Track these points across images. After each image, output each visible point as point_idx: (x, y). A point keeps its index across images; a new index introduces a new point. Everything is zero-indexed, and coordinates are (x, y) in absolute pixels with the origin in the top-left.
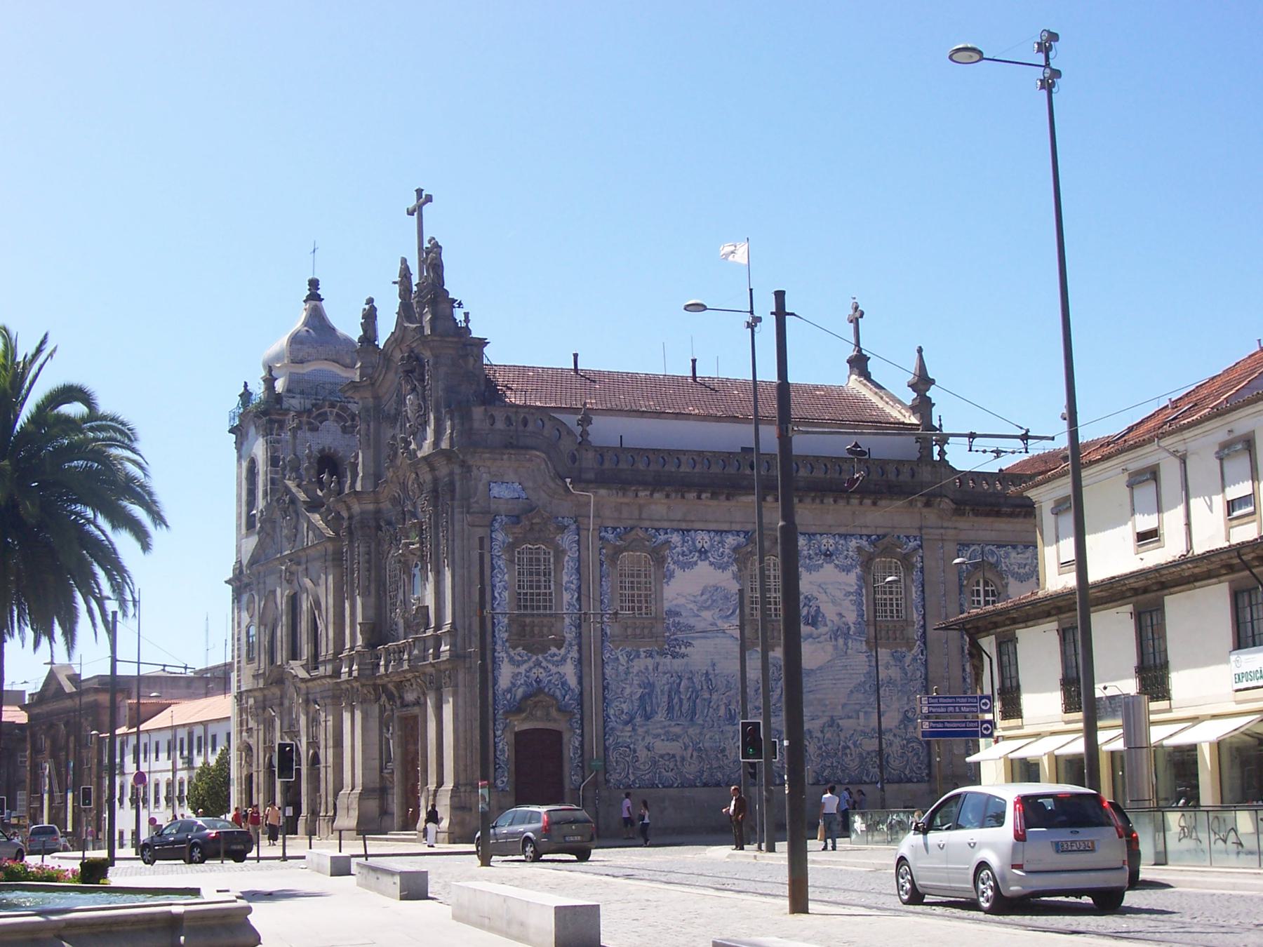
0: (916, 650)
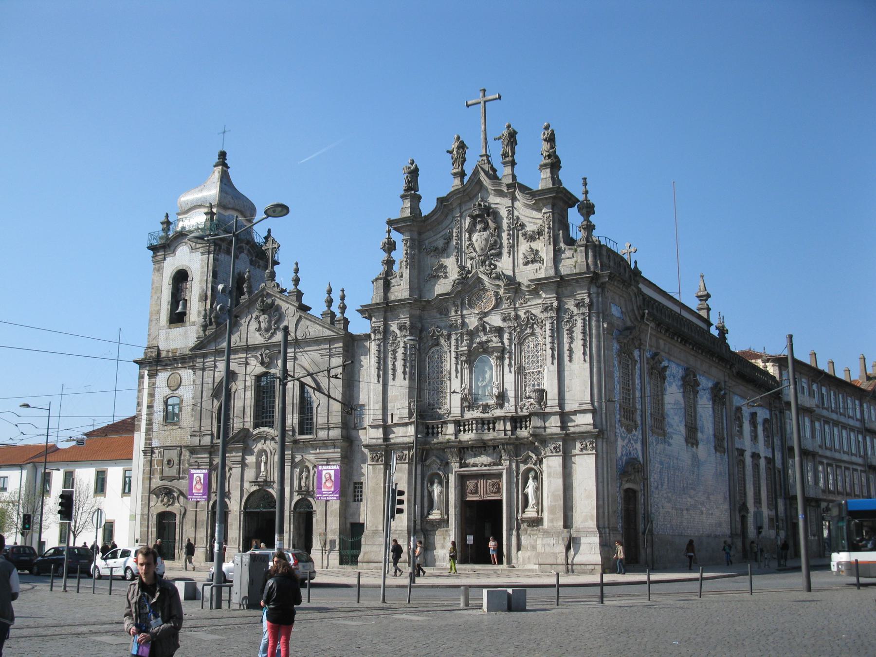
0: (726, 454)
